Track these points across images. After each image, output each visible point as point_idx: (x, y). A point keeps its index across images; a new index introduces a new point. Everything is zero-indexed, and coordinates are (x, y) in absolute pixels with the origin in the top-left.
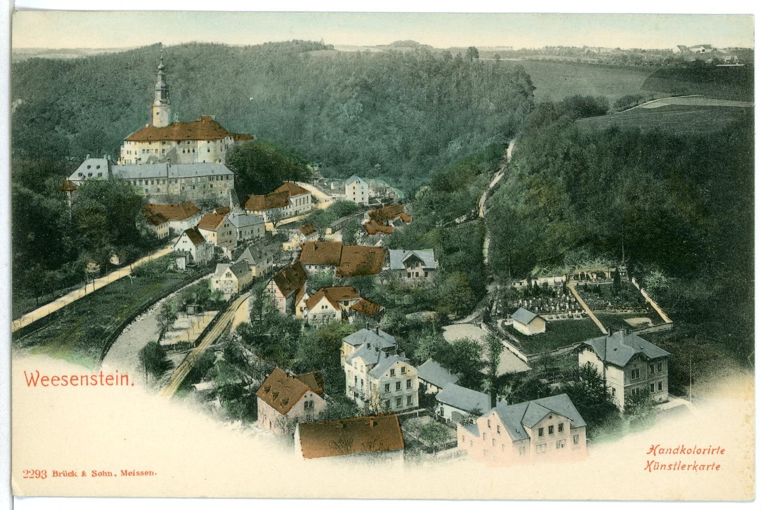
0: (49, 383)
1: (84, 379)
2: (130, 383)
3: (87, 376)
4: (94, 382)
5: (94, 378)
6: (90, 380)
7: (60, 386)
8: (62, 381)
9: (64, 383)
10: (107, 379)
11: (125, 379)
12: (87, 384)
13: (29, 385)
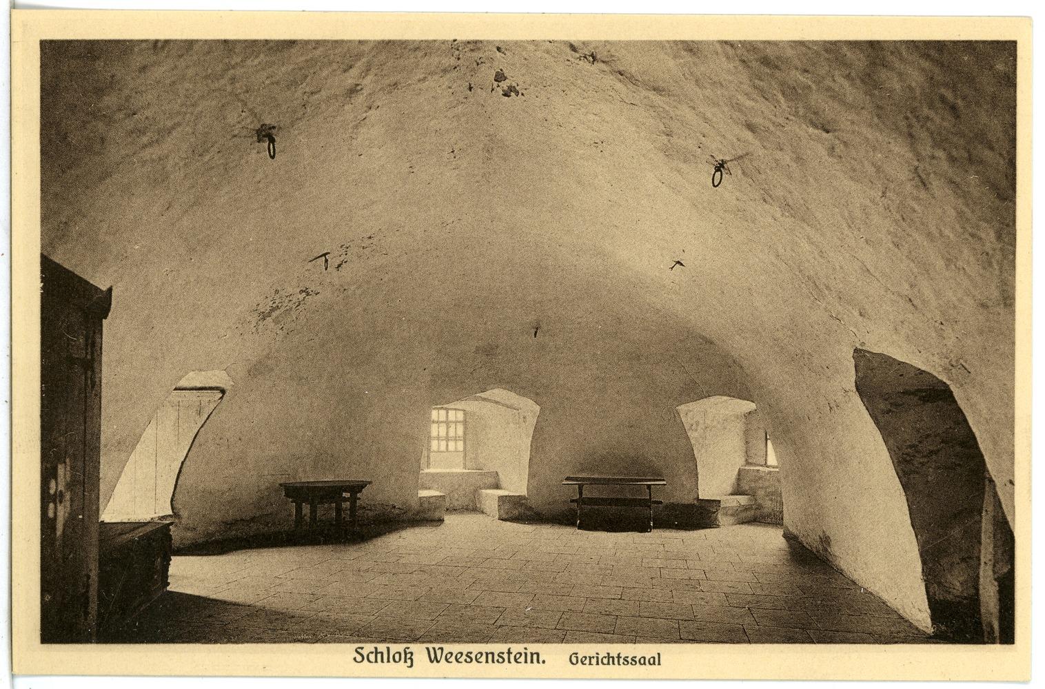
0: (453, 659)
1: (490, 656)
2: (541, 661)
3: (493, 654)
4: (501, 660)
5: (501, 655)
6: (496, 657)
7: (464, 663)
8: (464, 657)
9: (468, 660)
10: (515, 656)
11: (535, 656)
12: (493, 662)
13: (432, 662)
